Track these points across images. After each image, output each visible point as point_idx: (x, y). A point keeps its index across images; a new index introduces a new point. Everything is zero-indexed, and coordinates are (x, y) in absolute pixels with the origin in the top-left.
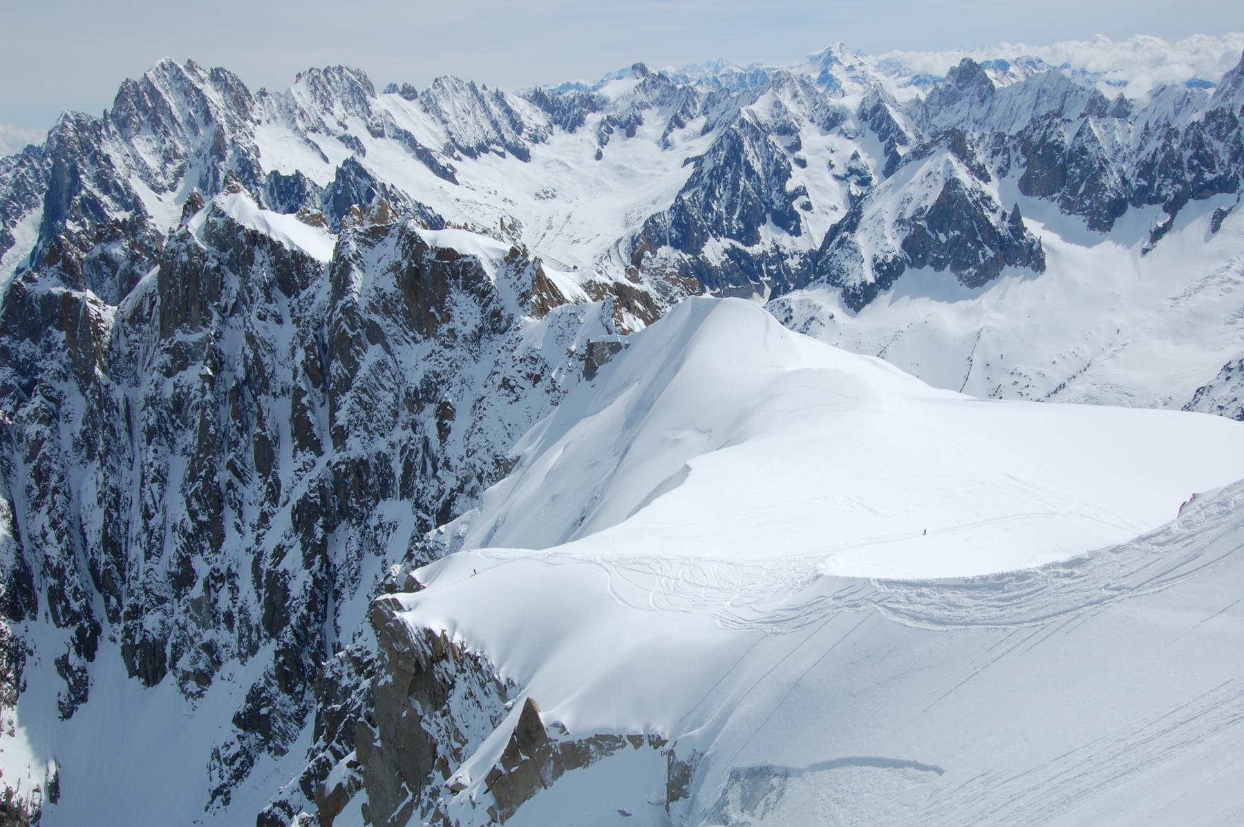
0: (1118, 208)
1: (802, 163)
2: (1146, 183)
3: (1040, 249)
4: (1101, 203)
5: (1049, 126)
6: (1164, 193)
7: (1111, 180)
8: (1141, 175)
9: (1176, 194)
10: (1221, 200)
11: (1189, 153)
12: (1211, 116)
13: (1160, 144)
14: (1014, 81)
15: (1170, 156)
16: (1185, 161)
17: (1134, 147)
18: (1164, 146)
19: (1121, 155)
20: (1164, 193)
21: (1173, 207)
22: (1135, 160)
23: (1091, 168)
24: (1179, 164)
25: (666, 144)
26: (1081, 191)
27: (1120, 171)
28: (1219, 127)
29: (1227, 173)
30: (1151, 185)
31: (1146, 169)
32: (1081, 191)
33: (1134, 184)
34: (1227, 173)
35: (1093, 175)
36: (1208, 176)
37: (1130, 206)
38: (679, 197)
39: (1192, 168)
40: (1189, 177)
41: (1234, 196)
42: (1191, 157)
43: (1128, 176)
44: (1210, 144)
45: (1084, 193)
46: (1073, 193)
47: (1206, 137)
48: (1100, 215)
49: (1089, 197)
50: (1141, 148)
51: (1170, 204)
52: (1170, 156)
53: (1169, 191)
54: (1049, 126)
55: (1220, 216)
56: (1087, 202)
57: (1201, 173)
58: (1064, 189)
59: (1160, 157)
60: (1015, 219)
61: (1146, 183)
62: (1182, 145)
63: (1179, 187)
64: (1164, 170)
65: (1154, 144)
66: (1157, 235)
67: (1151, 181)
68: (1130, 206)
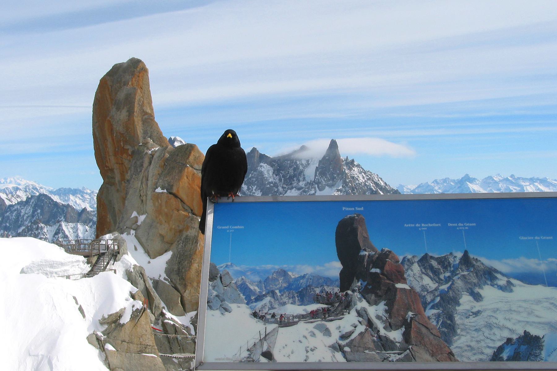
14: (19, 200)
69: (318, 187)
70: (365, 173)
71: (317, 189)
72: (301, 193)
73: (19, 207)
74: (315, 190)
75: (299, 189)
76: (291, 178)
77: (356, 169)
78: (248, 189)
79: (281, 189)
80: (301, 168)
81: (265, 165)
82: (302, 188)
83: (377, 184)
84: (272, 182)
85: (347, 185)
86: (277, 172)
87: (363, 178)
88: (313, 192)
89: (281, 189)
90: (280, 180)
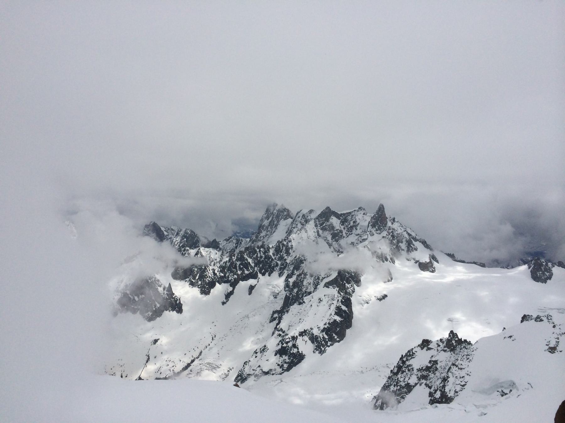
0: (212, 285)
2: (223, 275)
3: (180, 302)
4: (206, 283)
5: (184, 251)
6: (230, 279)
7: (210, 273)
8: (221, 271)
9: (235, 279)
10: (252, 282)
11: (238, 263)
12: (247, 249)
13: (227, 259)
15: (232, 263)
16: (238, 266)
17: (218, 260)
18: (230, 260)
19: (213, 263)
20: (230, 279)
21: (234, 284)
22: (218, 265)
23: (201, 268)
24: (235, 267)
26: (197, 278)
27: (214, 270)
28: (250, 253)
29: (253, 271)
30: (225, 275)
31: (222, 269)
32: (197, 278)
33: (218, 274)
34: (253, 271)
35: (203, 270)
36: (246, 272)
37: (217, 284)
39: (240, 269)
40: (239, 272)
41: (257, 280)
42: (240, 265)
43: (216, 272)
44: (247, 260)
45: (198, 278)
46: (194, 278)
47: (246, 256)
48: (205, 288)
49: (201, 280)
50: (221, 261)
51: (232, 283)
52: (232, 263)
53: (232, 278)
54: (184, 251)
55: (251, 288)
56: (200, 282)
57: (243, 271)
58: (191, 277)
59: (228, 264)
60: (170, 289)
61: (223, 275)
62: (236, 260)
63: (236, 276)
64: (229, 269)
65: (226, 259)
66: (228, 295)
67: (225, 274)
68: (217, 284)
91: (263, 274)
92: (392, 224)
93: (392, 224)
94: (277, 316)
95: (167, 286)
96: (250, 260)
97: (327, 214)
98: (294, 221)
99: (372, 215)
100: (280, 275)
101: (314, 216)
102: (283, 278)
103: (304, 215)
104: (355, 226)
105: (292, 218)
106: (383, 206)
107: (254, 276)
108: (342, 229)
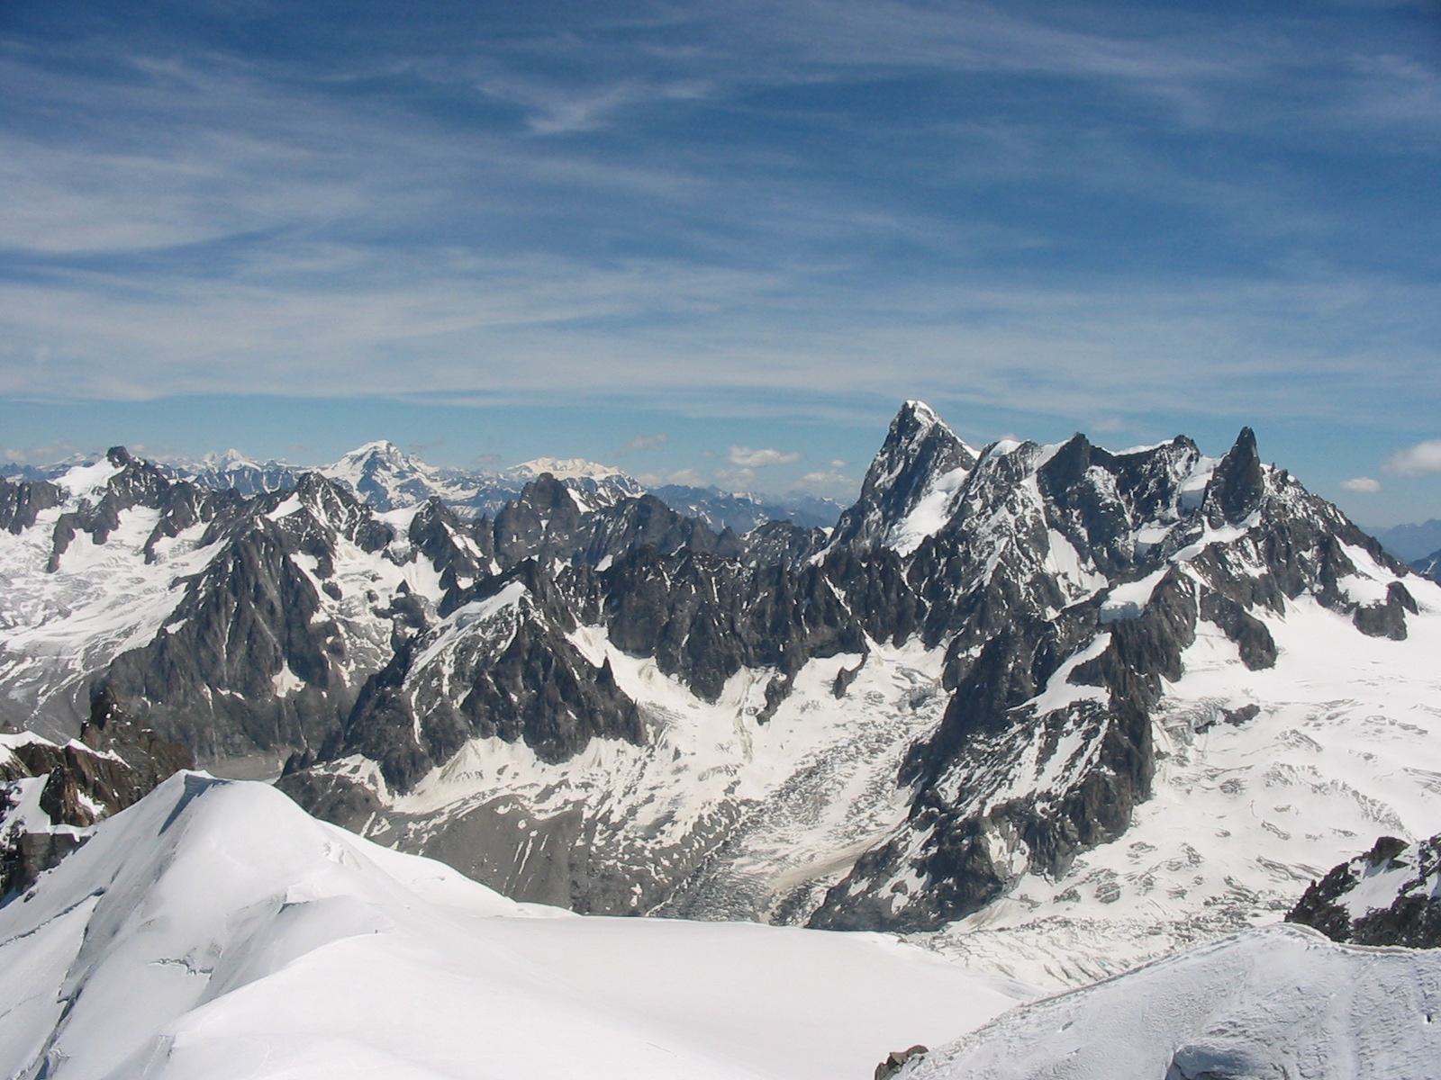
1: (1020, 764)
10: (849, 661)
21: (789, 665)
25: (149, 555)
38: (162, 631)
60: (605, 674)
69: (1209, 521)
70: (1308, 499)
71: (1206, 523)
72: (1172, 532)
73: (603, 517)
74: (1203, 525)
75: (1165, 523)
76: (1152, 500)
77: (1291, 490)
78: (1064, 515)
79: (1128, 518)
80: (1174, 479)
81: (1100, 469)
82: (1174, 520)
83: (1330, 522)
84: (1112, 504)
85: (1270, 522)
86: (1122, 486)
87: (1305, 509)
88: (1197, 529)
89: (1128, 518)
90: (1129, 502)
91: (880, 640)
92: (1280, 489)
93: (1280, 489)
94: (924, 764)
95: (599, 664)
96: (840, 594)
97: (1077, 455)
98: (972, 475)
99: (1219, 462)
100: (930, 643)
101: (1037, 461)
102: (940, 652)
103: (1003, 461)
104: (1165, 491)
105: (965, 469)
106: (1251, 434)
107: (850, 643)
108: (1122, 502)
